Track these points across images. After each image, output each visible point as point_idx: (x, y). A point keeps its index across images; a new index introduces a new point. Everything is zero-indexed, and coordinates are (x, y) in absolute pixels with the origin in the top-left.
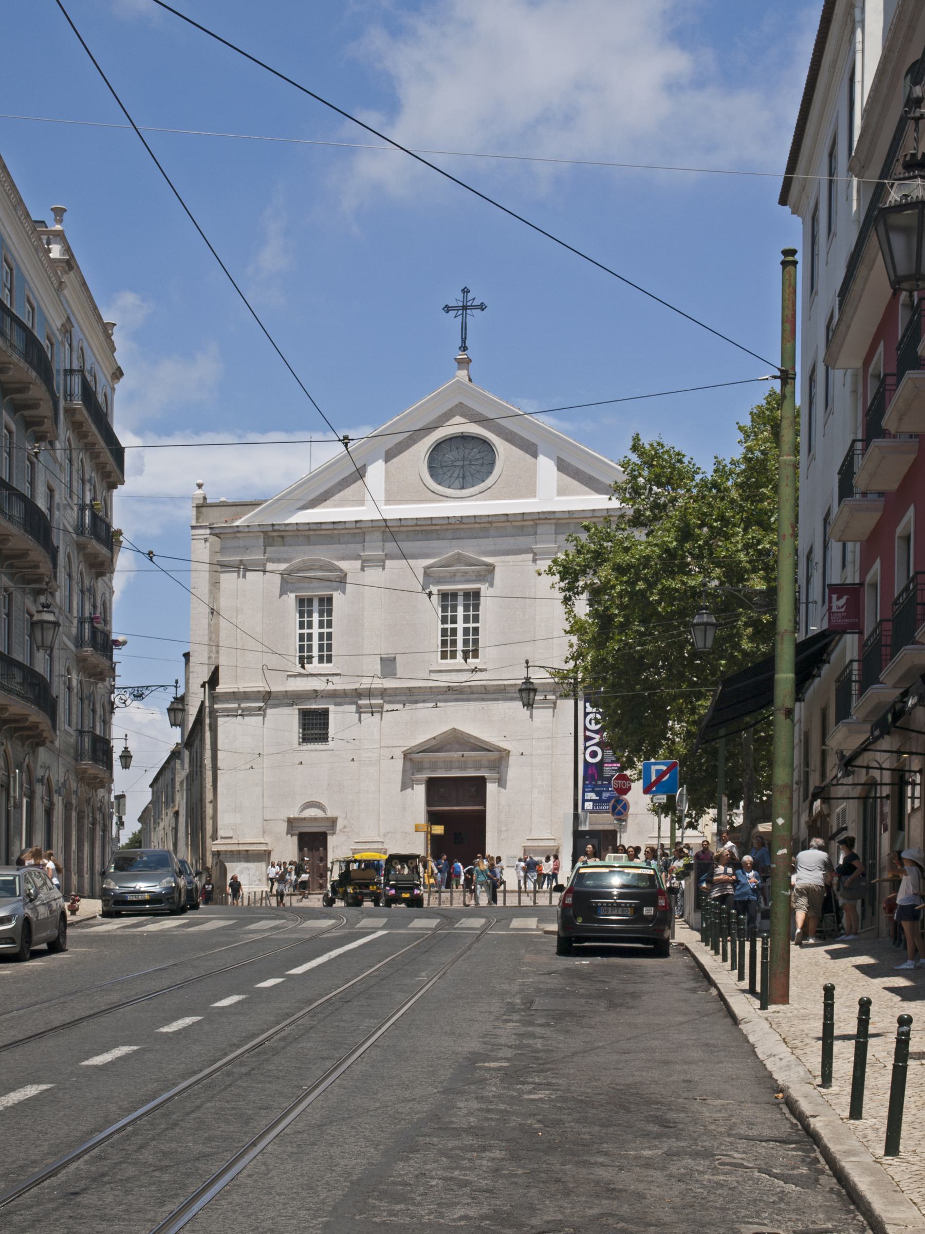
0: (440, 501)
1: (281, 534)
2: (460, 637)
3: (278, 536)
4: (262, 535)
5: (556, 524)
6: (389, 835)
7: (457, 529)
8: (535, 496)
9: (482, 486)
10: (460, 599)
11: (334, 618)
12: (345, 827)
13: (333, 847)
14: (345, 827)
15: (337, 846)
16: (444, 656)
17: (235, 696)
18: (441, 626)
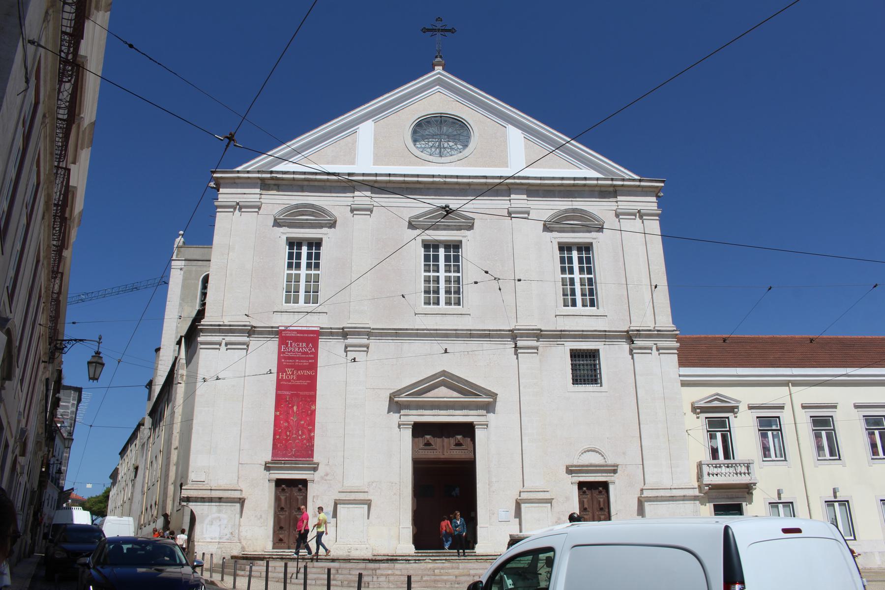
0: (422, 165)
1: (277, 182)
2: (442, 285)
3: (275, 185)
4: (259, 182)
5: (527, 190)
6: (374, 485)
7: (439, 189)
8: (507, 167)
9: (461, 155)
10: (442, 252)
11: (322, 262)
12: (327, 475)
13: (314, 497)
14: (327, 475)
15: (318, 496)
16: (427, 303)
17: (221, 330)
18: (424, 274)
